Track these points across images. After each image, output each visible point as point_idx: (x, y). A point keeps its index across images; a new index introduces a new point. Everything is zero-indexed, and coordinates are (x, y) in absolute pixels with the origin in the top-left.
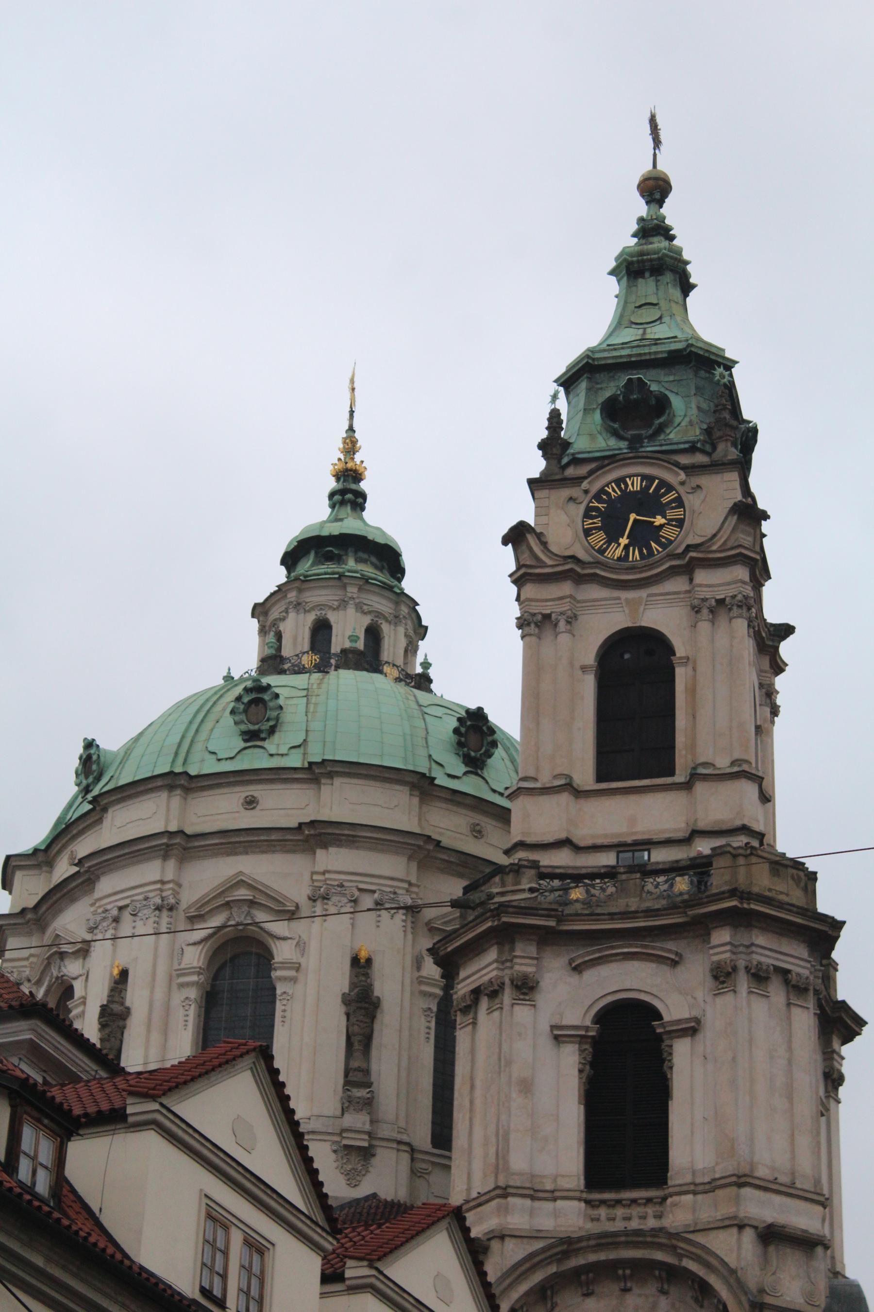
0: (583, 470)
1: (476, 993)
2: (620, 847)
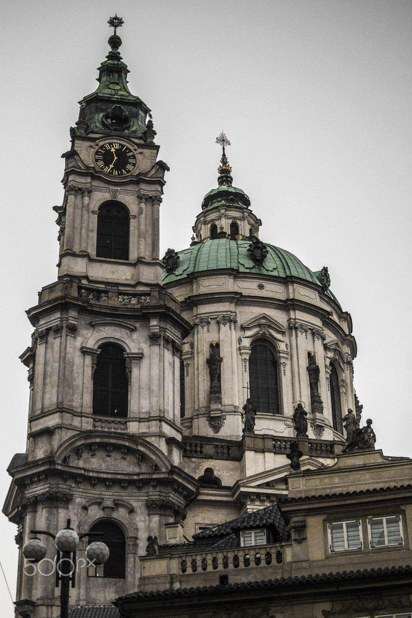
1: (48, 330)
2: (107, 284)
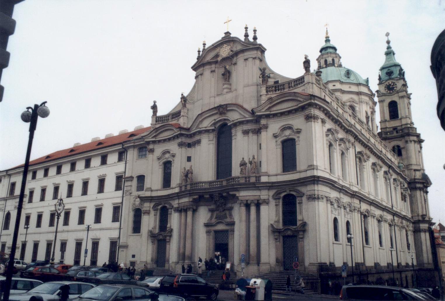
0: (384, 82)
